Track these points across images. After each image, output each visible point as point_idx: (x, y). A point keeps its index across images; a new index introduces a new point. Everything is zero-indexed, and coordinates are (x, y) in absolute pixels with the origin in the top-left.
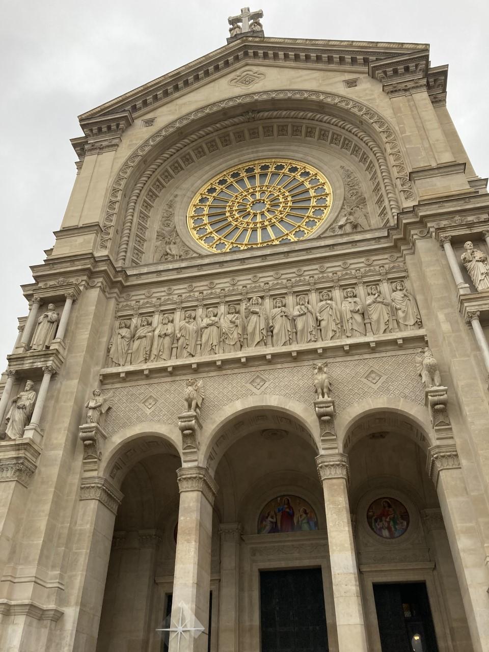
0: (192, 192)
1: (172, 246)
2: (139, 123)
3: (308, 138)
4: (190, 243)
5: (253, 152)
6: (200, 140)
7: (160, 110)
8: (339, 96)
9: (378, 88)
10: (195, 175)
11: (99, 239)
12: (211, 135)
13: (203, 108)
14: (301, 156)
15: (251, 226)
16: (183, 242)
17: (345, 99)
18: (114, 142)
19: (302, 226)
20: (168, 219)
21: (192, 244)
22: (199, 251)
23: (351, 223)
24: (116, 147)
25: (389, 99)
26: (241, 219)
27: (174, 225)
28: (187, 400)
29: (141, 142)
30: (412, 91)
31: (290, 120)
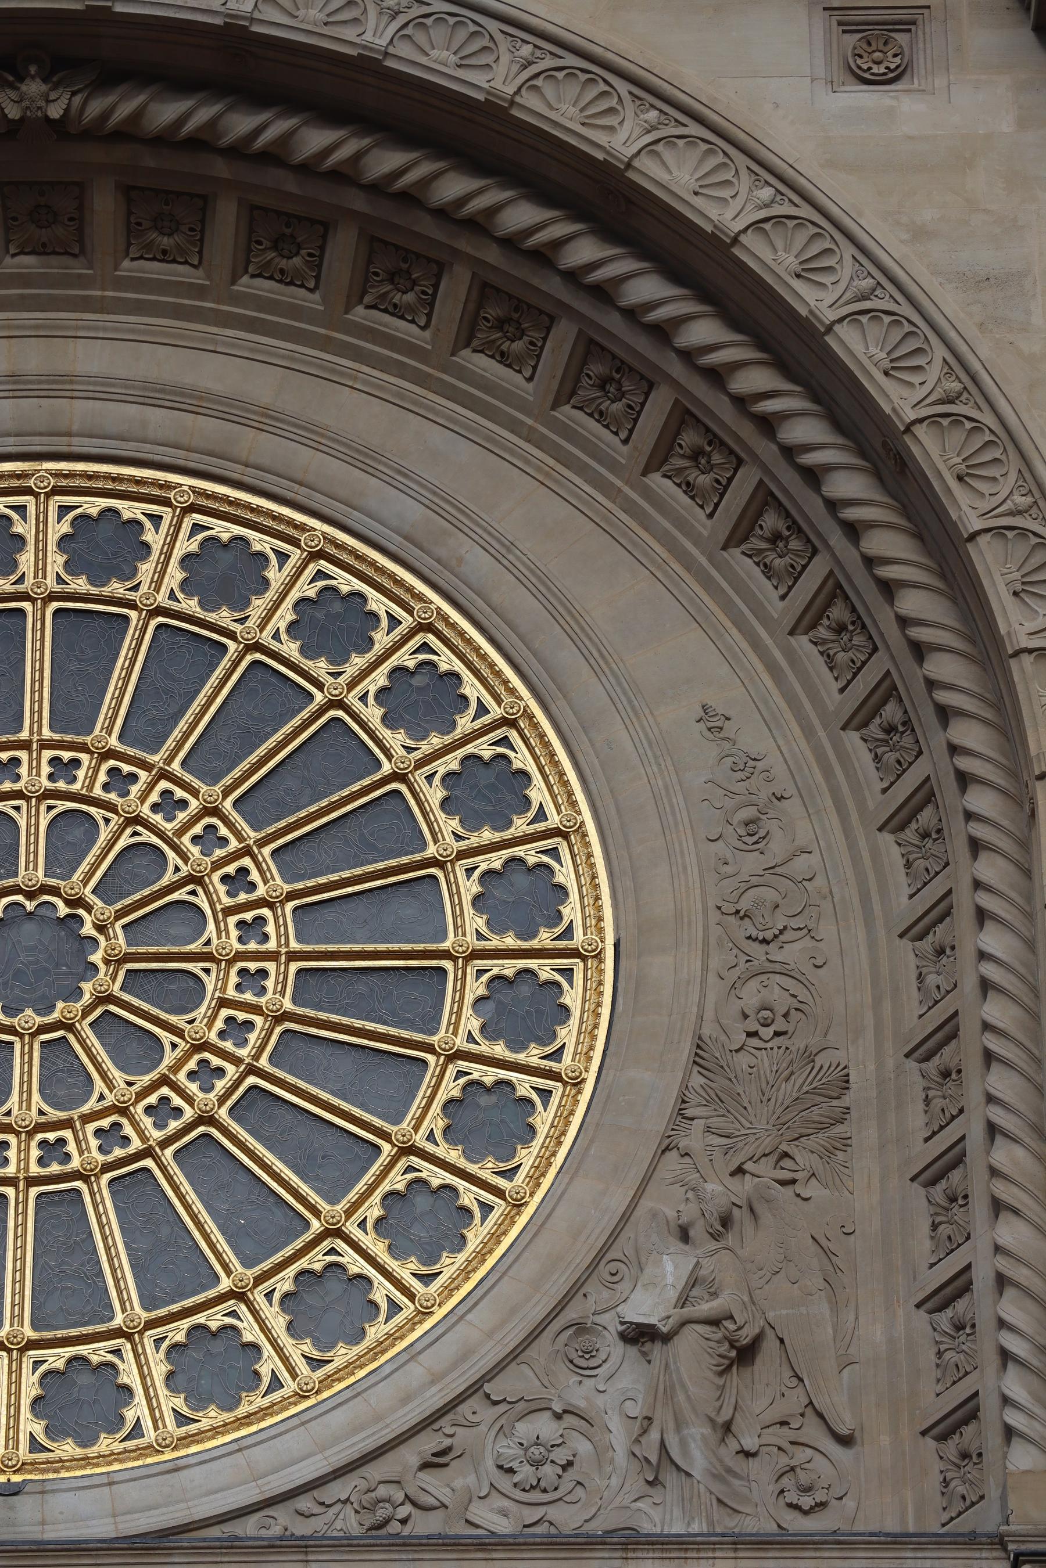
8: (764, 167)
14: (410, 511)
17: (805, 211)
19: (352, 1228)
23: (714, 1322)
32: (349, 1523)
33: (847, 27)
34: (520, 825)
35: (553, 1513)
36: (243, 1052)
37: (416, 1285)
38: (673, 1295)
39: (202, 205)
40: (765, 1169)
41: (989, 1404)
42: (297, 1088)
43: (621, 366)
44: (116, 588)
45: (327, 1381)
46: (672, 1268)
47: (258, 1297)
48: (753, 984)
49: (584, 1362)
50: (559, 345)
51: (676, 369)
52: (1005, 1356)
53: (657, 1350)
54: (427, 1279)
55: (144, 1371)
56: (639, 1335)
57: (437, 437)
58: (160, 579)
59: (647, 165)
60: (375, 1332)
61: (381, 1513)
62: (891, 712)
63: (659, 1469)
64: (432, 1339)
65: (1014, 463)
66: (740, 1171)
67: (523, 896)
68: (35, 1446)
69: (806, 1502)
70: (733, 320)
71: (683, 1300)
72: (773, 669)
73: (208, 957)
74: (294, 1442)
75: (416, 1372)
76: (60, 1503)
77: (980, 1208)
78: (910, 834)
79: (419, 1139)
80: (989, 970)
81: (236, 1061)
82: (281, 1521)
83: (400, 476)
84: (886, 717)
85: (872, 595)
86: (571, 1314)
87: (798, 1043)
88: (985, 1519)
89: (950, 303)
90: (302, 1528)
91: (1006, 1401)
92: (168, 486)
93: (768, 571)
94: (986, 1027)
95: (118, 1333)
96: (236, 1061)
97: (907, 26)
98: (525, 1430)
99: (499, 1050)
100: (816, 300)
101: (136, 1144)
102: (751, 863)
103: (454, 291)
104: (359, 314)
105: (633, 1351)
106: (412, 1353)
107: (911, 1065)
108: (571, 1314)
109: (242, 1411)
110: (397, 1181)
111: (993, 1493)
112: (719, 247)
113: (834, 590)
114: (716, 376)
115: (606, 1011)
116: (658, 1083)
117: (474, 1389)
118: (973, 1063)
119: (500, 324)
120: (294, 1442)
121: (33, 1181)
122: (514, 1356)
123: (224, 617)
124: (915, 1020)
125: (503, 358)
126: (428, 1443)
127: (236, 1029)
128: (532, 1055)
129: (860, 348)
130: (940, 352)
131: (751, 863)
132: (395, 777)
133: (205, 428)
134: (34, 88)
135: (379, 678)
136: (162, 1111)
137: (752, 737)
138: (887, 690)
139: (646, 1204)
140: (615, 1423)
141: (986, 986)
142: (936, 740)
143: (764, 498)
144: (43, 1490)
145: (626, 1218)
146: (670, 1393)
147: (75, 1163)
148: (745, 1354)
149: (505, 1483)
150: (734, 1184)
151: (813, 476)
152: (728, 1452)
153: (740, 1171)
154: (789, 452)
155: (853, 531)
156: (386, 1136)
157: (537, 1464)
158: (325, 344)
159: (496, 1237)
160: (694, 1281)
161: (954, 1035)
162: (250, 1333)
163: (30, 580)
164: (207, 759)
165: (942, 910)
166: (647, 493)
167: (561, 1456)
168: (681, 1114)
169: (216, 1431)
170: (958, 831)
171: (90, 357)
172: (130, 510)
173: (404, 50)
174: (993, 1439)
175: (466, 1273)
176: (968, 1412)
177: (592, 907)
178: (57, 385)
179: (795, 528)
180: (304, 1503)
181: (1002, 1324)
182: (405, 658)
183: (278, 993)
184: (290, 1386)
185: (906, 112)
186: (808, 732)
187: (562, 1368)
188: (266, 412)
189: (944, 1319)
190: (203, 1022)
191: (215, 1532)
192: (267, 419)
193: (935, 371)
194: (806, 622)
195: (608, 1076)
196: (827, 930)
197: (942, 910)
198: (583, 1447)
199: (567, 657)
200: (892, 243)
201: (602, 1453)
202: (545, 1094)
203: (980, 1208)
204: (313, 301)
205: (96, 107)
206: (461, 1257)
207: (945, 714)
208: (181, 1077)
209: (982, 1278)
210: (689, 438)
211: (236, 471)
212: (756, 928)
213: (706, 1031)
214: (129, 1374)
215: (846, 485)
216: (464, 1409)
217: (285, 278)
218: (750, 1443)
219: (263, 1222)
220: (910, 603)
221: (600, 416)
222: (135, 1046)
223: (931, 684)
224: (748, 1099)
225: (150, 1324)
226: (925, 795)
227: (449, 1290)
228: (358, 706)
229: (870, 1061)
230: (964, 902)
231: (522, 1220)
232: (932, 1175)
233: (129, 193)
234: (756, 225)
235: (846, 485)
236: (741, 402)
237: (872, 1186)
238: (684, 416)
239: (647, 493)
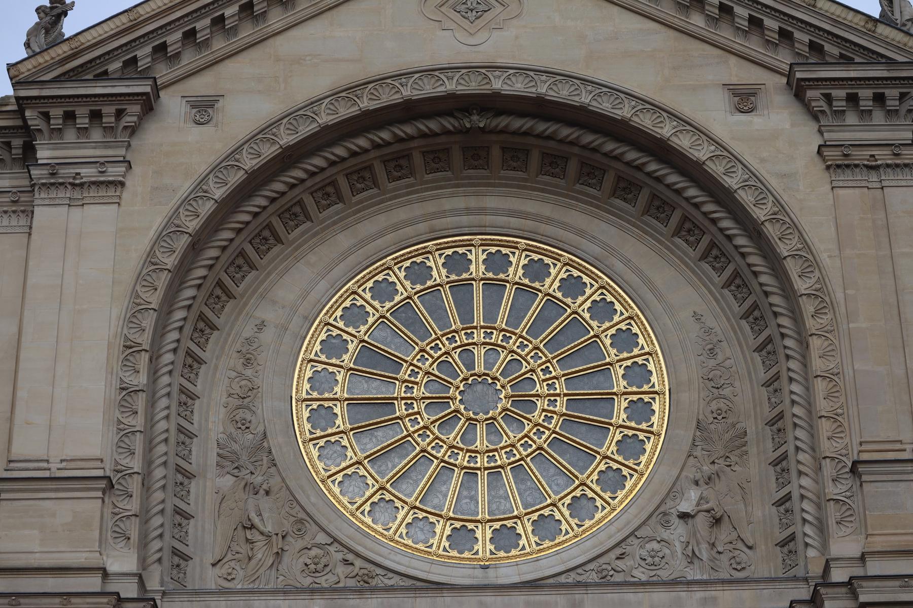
0: (306, 318)
1: (265, 503)
2: (172, 103)
3: (618, 202)
4: (308, 497)
5: (468, 211)
6: (334, 170)
7: (230, 67)
8: (712, 140)
9: (807, 137)
10: (312, 258)
11: (108, 510)
12: (364, 158)
13: (352, 90)
14: (597, 250)
15: (462, 459)
16: (288, 488)
17: (725, 153)
18: (114, 172)
19: (588, 482)
20: (245, 398)
21: (313, 499)
22: (331, 528)
23: (708, 511)
24: (119, 189)
25: (829, 187)
26: (436, 431)
27: (261, 429)
29: (185, 187)
30: (888, 177)
31: (576, 150)
32: (594, 577)
33: (735, 95)
34: (636, 351)
35: (658, 572)
36: (551, 426)
37: (610, 500)
38: (694, 503)
39: (527, 152)
40: (721, 461)
41: (799, 536)
43: (665, 202)
44: (502, 276)
45: (584, 532)
46: (693, 494)
47: (560, 505)
48: (714, 402)
49: (666, 525)
50: (643, 197)
51: (684, 204)
52: (805, 521)
53: (690, 521)
54: (614, 498)
55: (524, 529)
56: (684, 516)
57: (604, 225)
58: (515, 272)
59: (674, 139)
60: (598, 516)
61: (604, 573)
62: (756, 313)
63: (692, 558)
64: (617, 518)
65: (797, 234)
66: (713, 462)
67: (638, 373)
68: (492, 553)
69: (739, 567)
70: (701, 187)
71: (698, 504)
73: (538, 396)
74: (574, 552)
75: (613, 529)
76: (502, 571)
77: (794, 474)
78: (764, 353)
79: (609, 454)
80: (794, 397)
81: (549, 429)
82: (572, 578)
83: (593, 239)
84: (755, 315)
85: (750, 276)
86: (662, 509)
87: (730, 421)
88: (800, 572)
89: (774, 183)
90: (579, 578)
91: (805, 534)
92: (517, 243)
93: (714, 268)
94: (794, 415)
95: (516, 517)
96: (549, 429)
97: (754, 94)
98: (649, 546)
99: (633, 424)
100: (731, 182)
101: (518, 457)
102: (712, 363)
103: (609, 180)
104: (578, 187)
105: (681, 521)
106: (611, 522)
107: (767, 427)
108: (662, 509)
109: (557, 541)
110: (602, 467)
111: (802, 564)
112: (698, 165)
113: (736, 274)
114: (697, 206)
115: (667, 411)
116: (686, 435)
117: (632, 534)
118: (790, 427)
119: (624, 189)
120: (574, 552)
121: (486, 469)
122: (644, 523)
123: (537, 285)
124: (768, 413)
125: (625, 200)
126: (618, 551)
127: (548, 419)
128: (644, 426)
129: (746, 197)
130: (771, 198)
131: (712, 363)
132: (595, 336)
133: (529, 224)
134: (475, 118)
135: (588, 304)
137: (710, 322)
138: (755, 306)
139: (684, 474)
140: (677, 544)
141: (793, 402)
142: (772, 323)
143: (712, 245)
144: (496, 567)
145: (678, 478)
146: (695, 534)
147: (499, 463)
148: (717, 521)
149: (643, 563)
150: (712, 467)
151: (729, 238)
152: (714, 552)
153: (713, 462)
154: (721, 230)
155: (743, 255)
156: (598, 453)
157: (653, 557)
158: (566, 196)
159: (635, 485)
160: (701, 498)
161: (782, 418)
162: (558, 516)
163: (474, 274)
165: (777, 377)
166: (673, 243)
167: (660, 554)
168: (694, 445)
169: (549, 548)
170: (781, 353)
171: (491, 202)
172: (504, 251)
173: (594, 103)
174: (801, 547)
175: (626, 496)
176: (792, 538)
178: (482, 211)
179: (723, 254)
180: (580, 571)
181: (803, 510)
182: (596, 297)
183: (561, 406)
184: (571, 534)
185: (756, 122)
186: (728, 319)
187: (659, 527)
188: (548, 218)
189: (782, 509)
191: (551, 581)
192: (548, 221)
193: (770, 205)
194: (727, 285)
195: (669, 432)
196: (737, 384)
197: (777, 377)
198: (667, 551)
199: (649, 296)
200: (754, 164)
201: (673, 553)
202: (648, 438)
203: (794, 474)
204: (562, 183)
205: (494, 124)
206: (624, 492)
207: (776, 314)
208: (531, 434)
209: (795, 495)
210: (687, 225)
211: (539, 238)
212: (714, 384)
213: (700, 418)
214: (520, 530)
215: (740, 241)
216: (629, 540)
217: (553, 175)
218: (720, 549)
220: (764, 279)
221: (657, 218)
223: (771, 305)
224: (712, 439)
225: (526, 514)
226: (769, 340)
227: (621, 502)
228: (582, 313)
229: (753, 427)
230: (784, 375)
231: (644, 479)
232: (775, 463)
233: (504, 149)
234: (710, 158)
235: (740, 241)
236: (705, 214)
237: (756, 466)
238: (685, 218)
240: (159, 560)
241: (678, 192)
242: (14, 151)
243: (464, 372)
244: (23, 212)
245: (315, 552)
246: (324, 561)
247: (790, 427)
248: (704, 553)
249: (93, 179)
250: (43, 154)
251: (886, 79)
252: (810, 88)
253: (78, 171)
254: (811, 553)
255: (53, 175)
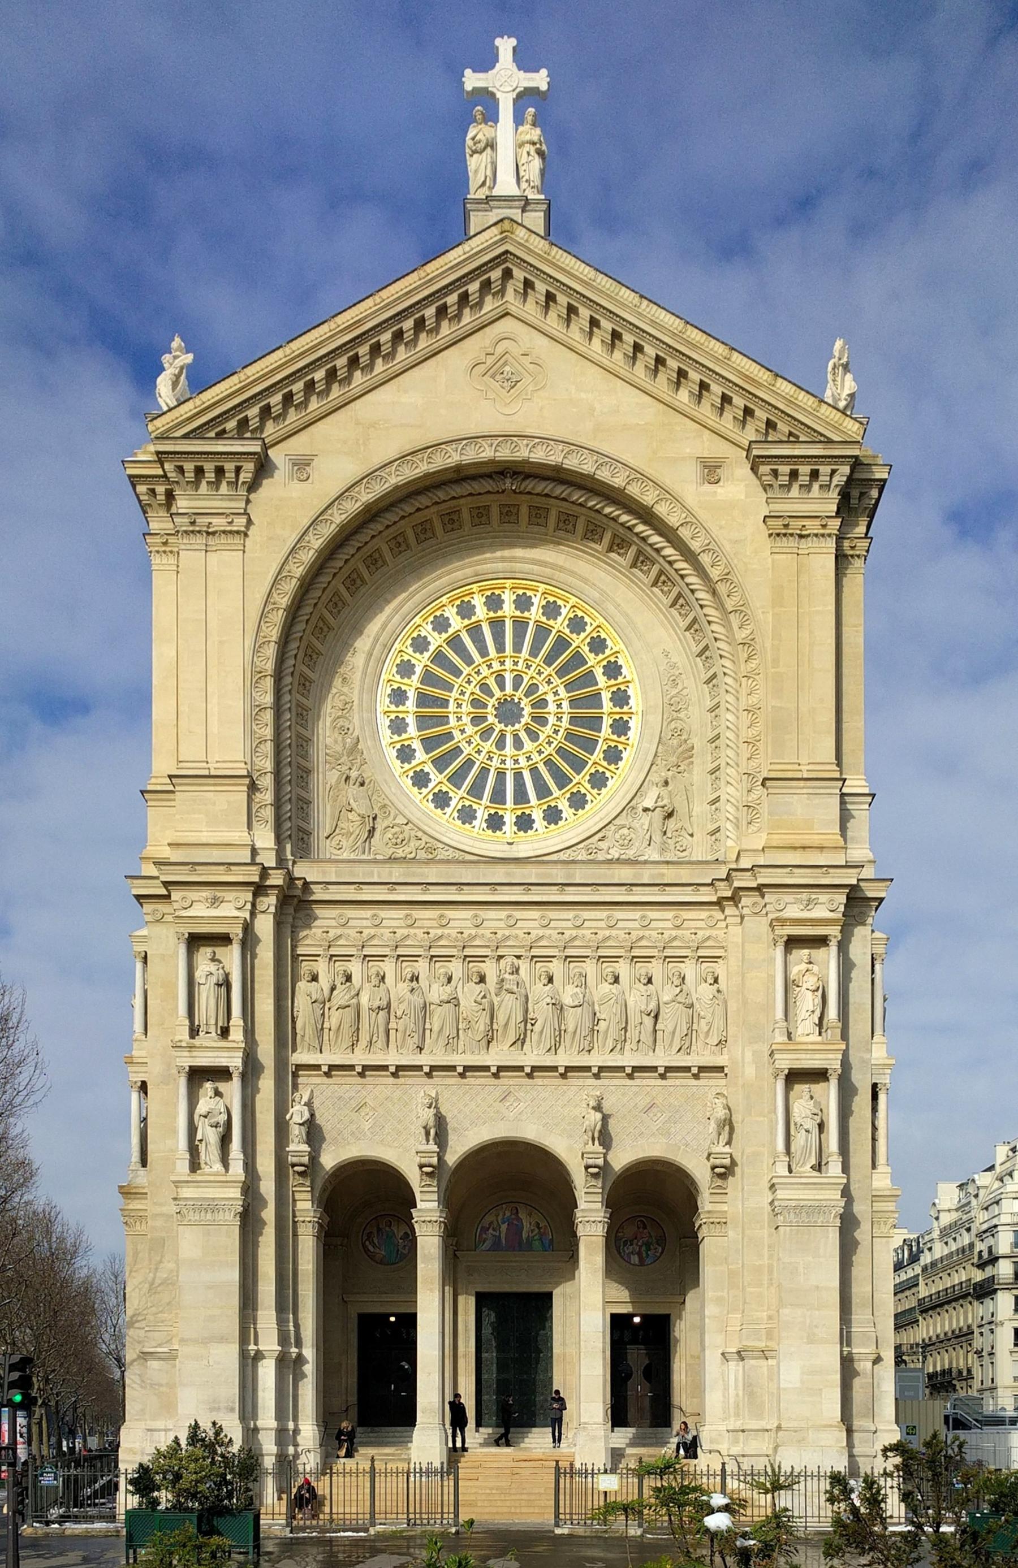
4: (390, 787)
22: (406, 812)
28: (425, 1128)
42: (570, 747)
56: (646, 810)
72: (680, 639)
87: (683, 738)
117: (610, 822)
131: (674, 692)
136: (540, 752)
148: (670, 815)
149: (617, 844)
164: (549, 661)
165: (717, 706)
166: (652, 592)
176: (718, 830)
177: (636, 702)
186: (687, 656)
188: (561, 567)
190: (548, 730)
197: (717, 706)
203: (723, 783)
219: (562, 781)
222: (534, 736)
232: (712, 772)
239: (652, 592)
240: (290, 836)
241: (658, 551)
242: (158, 497)
243: (498, 693)
244: (171, 552)
245: (393, 831)
246: (401, 836)
247: (723, 747)
248: (657, 837)
249: (222, 528)
250: (182, 504)
251: (822, 457)
252: (763, 463)
253: (210, 520)
254: (730, 843)
255: (193, 523)
